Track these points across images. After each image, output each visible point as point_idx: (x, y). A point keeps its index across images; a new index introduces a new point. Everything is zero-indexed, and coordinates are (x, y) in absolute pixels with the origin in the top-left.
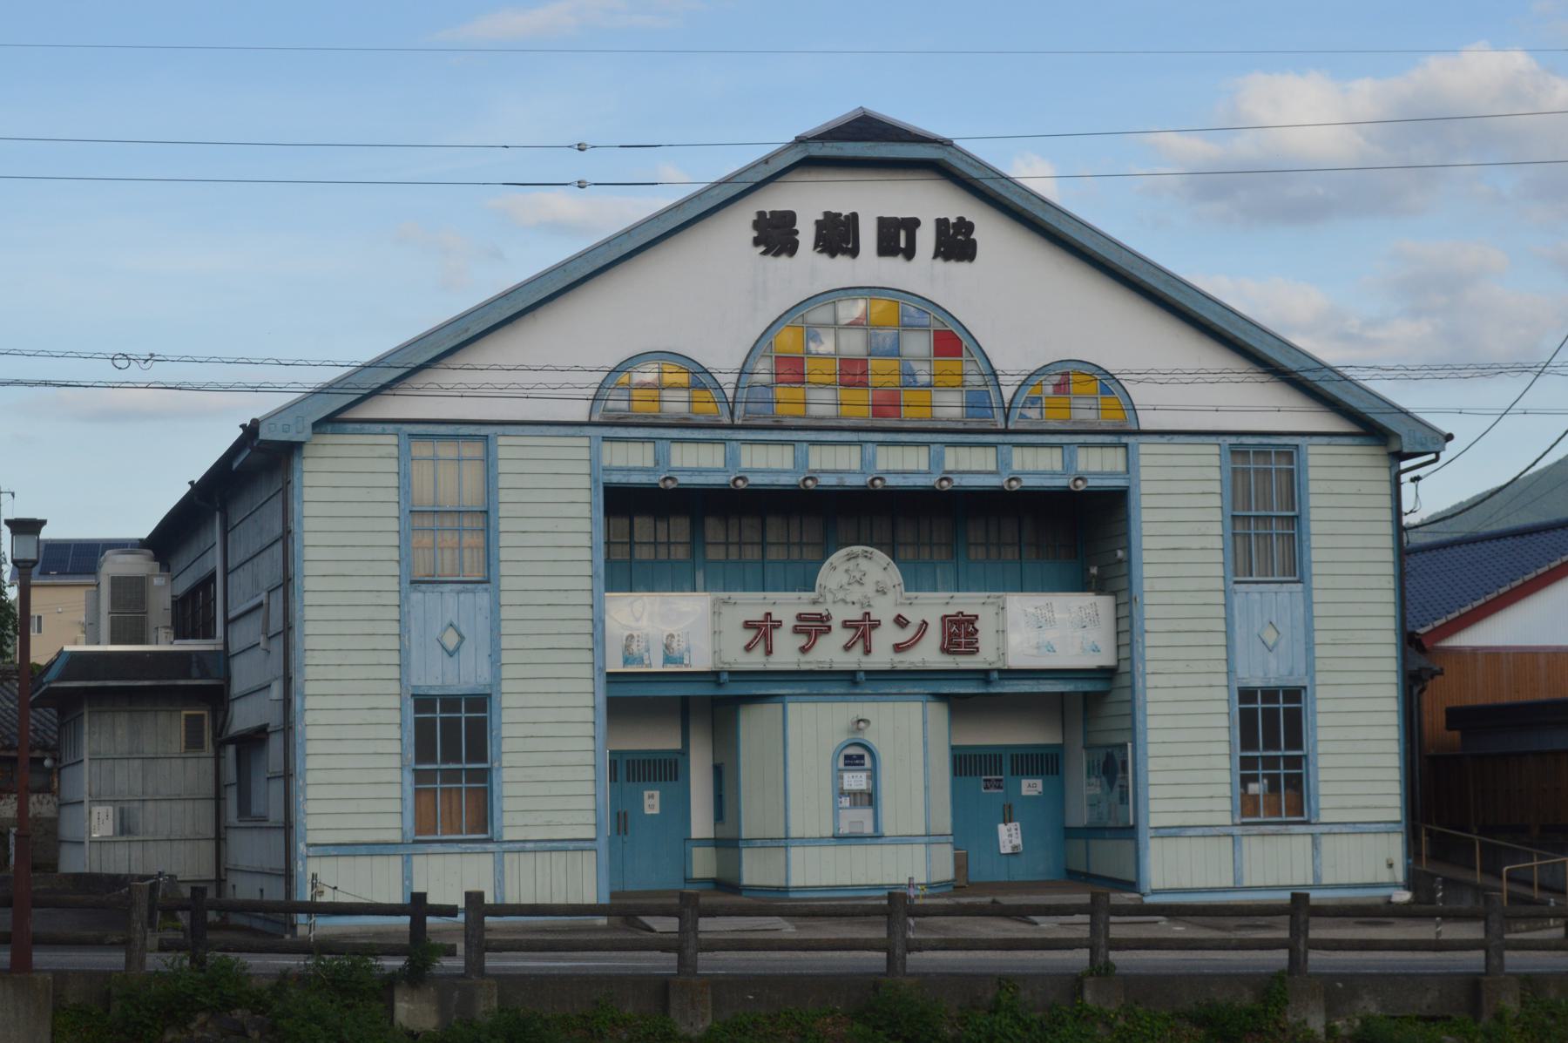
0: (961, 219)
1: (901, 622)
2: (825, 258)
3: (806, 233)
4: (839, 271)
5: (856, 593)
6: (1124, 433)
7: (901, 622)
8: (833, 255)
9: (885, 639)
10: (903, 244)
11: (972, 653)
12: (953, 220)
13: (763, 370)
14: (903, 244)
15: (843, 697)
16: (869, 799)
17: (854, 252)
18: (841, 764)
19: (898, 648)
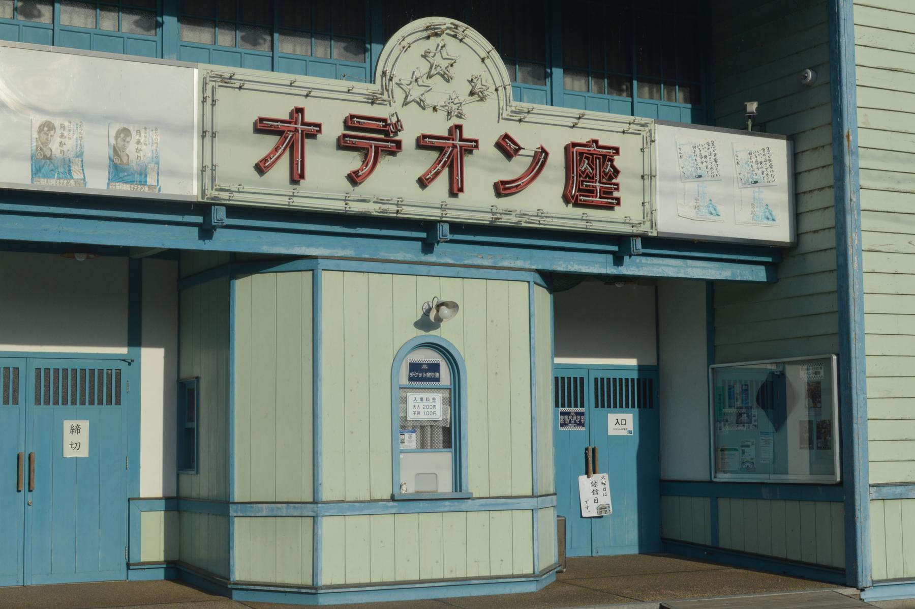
1: (507, 147)
5: (439, 93)
7: (507, 147)
9: (481, 173)
11: (610, 207)
15: (408, 267)
16: (450, 436)
18: (403, 377)
19: (503, 189)
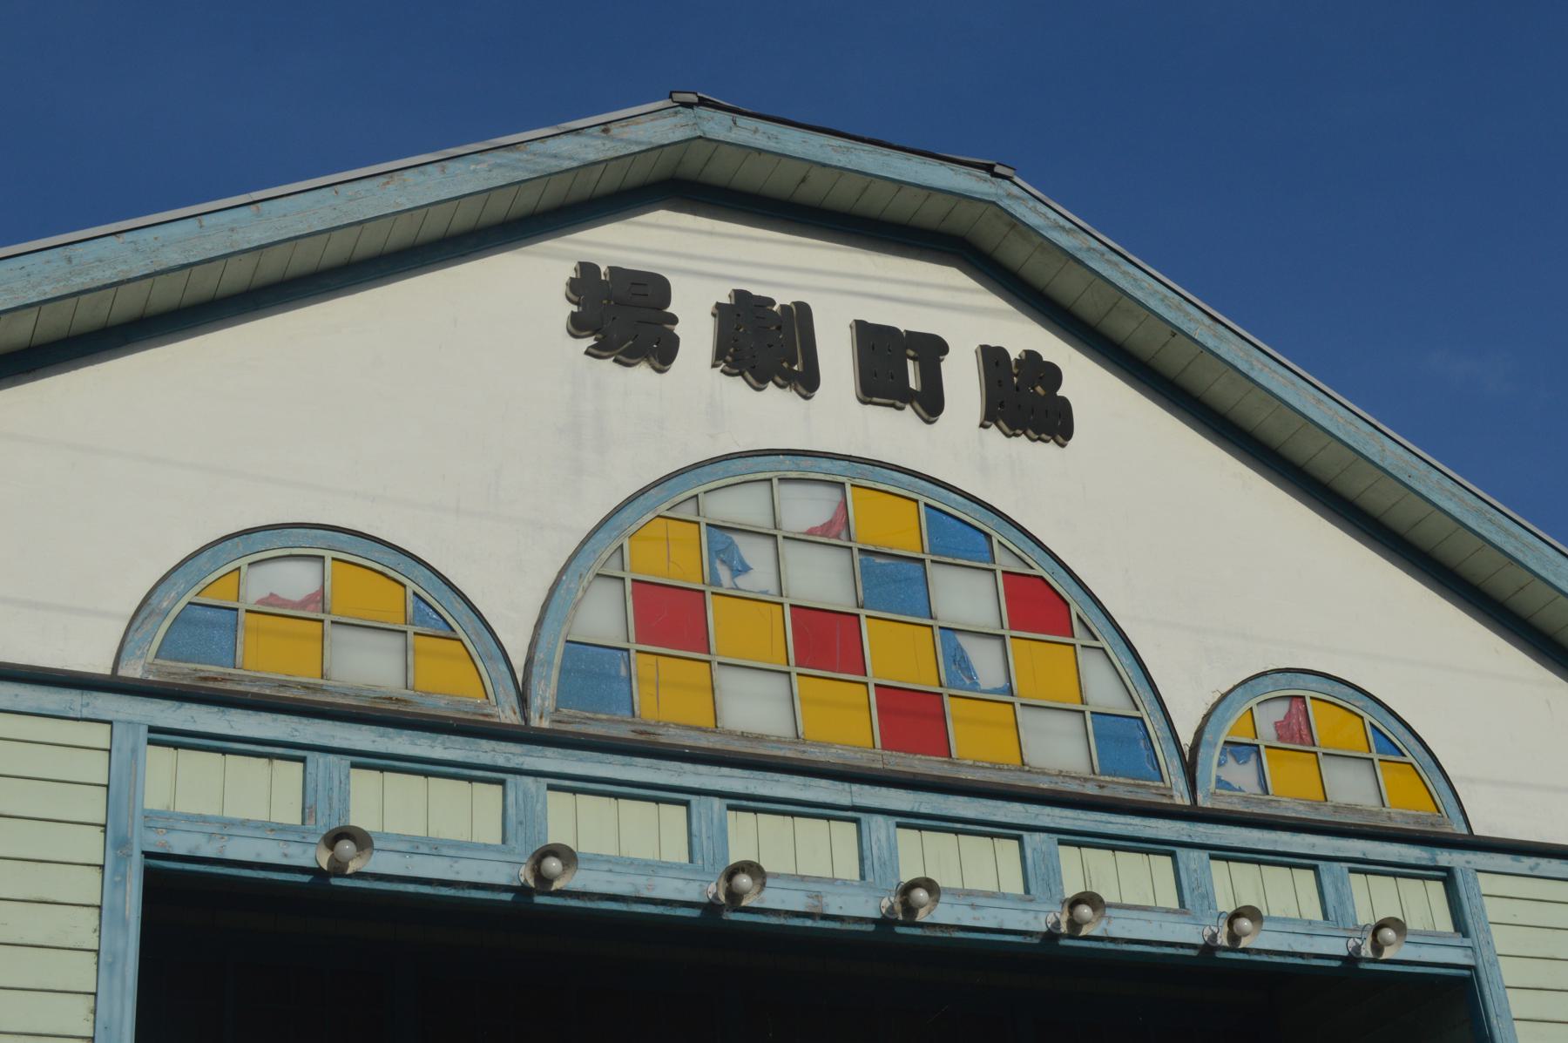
0: (1032, 357)
2: (738, 387)
3: (696, 331)
4: (768, 416)
6: (1440, 844)
8: (760, 379)
10: (914, 382)
12: (1014, 354)
13: (603, 617)
14: (914, 382)
17: (808, 382)
